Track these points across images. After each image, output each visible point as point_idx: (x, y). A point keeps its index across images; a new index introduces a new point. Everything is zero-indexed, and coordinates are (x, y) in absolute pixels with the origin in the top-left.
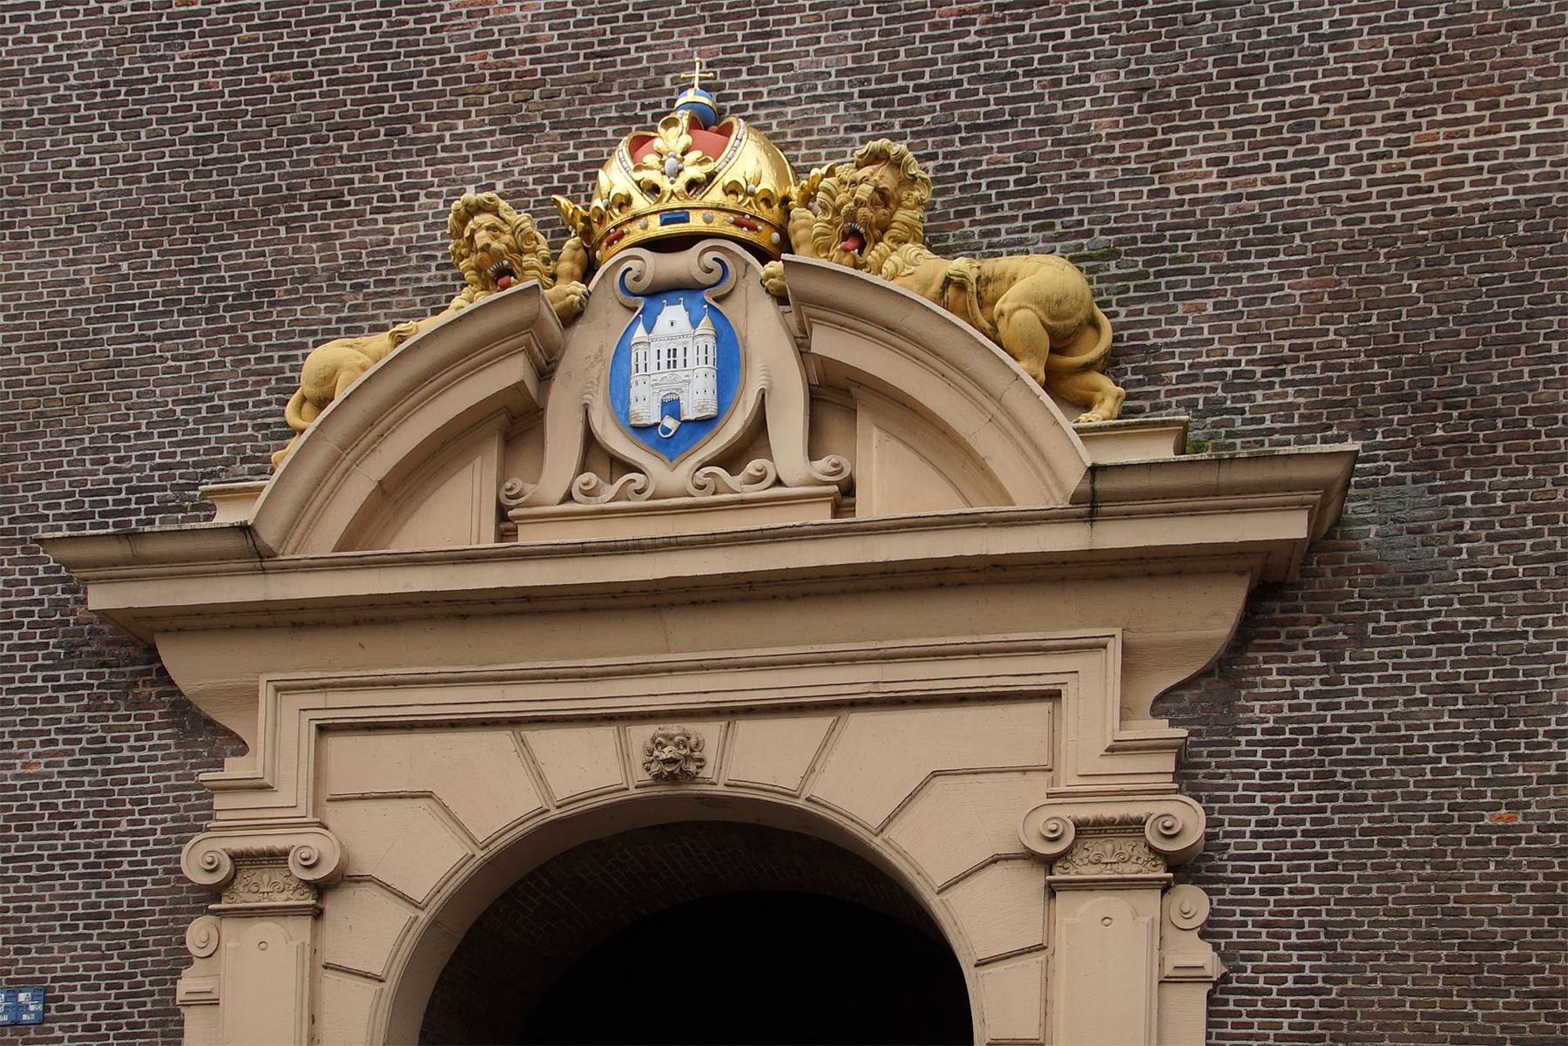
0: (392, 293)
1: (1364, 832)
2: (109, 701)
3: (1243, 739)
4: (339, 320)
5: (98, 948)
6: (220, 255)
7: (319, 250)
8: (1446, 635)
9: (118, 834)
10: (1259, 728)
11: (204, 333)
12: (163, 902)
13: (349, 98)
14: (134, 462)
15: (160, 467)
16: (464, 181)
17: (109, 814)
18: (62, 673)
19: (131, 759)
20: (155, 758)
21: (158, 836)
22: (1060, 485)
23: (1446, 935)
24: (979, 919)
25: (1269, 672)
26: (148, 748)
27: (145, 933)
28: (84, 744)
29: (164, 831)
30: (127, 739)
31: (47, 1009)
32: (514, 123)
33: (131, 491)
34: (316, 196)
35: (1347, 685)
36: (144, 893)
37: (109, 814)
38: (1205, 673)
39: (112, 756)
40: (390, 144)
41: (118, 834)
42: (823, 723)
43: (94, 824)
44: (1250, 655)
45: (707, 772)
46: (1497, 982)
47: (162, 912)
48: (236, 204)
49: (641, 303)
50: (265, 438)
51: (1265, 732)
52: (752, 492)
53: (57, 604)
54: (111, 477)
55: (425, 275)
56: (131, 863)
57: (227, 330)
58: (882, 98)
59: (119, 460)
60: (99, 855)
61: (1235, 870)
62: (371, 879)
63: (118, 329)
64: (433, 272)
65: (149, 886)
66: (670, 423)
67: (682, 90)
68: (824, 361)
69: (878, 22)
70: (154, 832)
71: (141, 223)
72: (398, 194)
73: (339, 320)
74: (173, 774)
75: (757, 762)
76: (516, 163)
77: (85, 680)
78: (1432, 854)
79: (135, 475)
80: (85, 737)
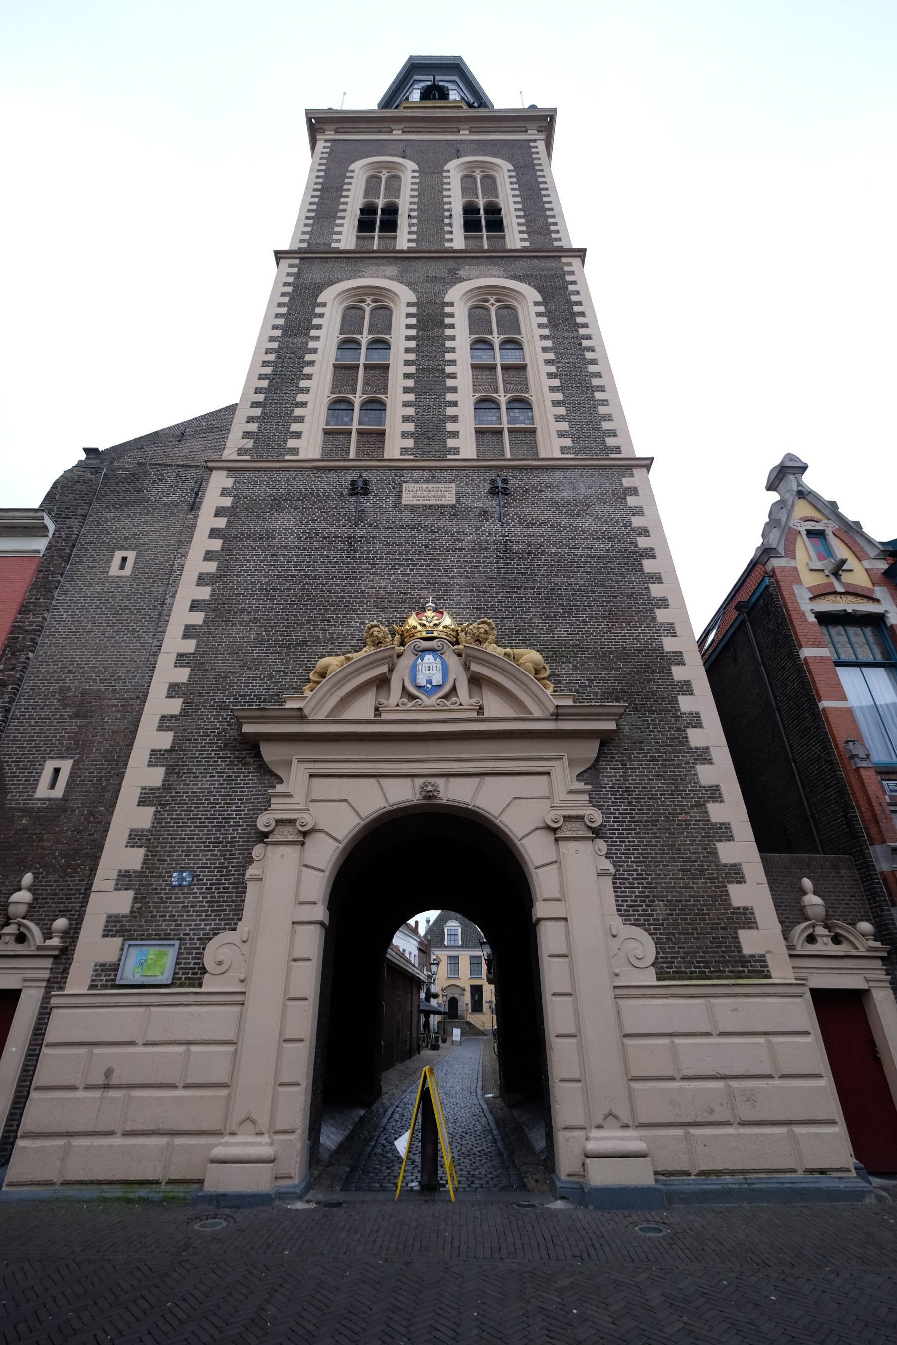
1: (646, 821)
5: (216, 855)
8: (653, 759)
22: (547, 709)
23: (679, 858)
24: (535, 850)
26: (247, 780)
31: (193, 880)
38: (589, 768)
42: (475, 780)
43: (223, 807)
46: (696, 874)
49: (419, 653)
52: (453, 707)
53: (225, 730)
58: (479, 609)
60: (223, 819)
62: (323, 831)
66: (429, 686)
68: (474, 672)
70: (244, 811)
75: (455, 792)
78: (667, 829)
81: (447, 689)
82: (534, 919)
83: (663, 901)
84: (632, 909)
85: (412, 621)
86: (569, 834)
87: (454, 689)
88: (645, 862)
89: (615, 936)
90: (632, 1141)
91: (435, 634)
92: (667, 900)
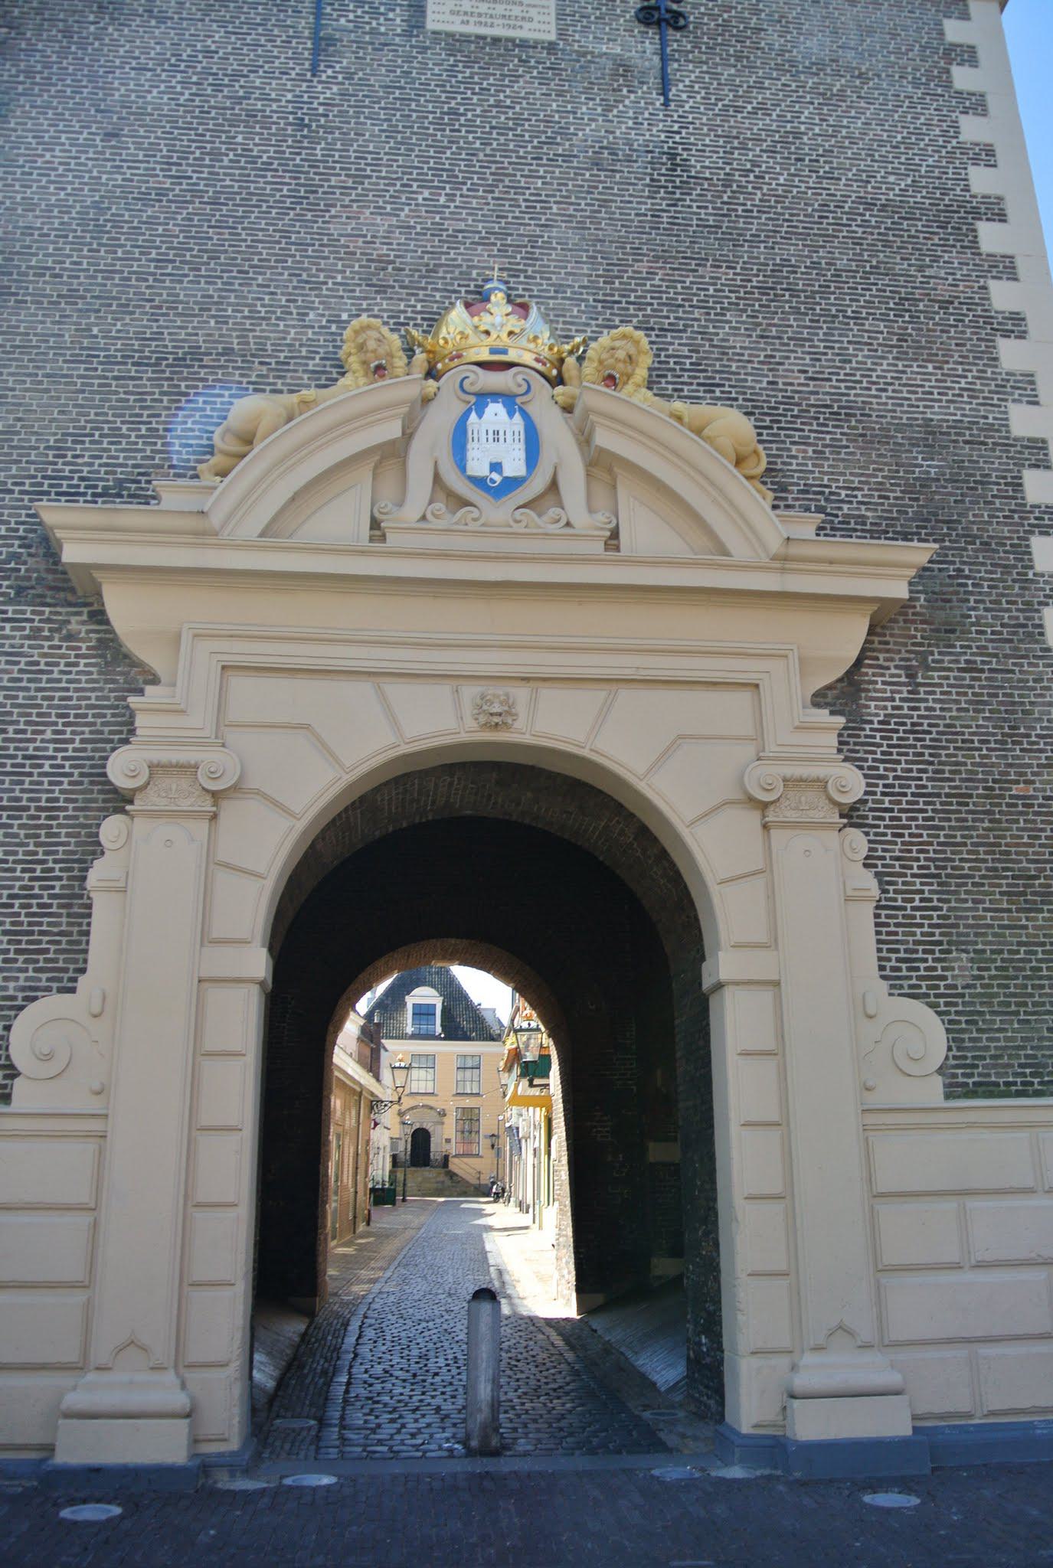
0: (288, 371)
1: (947, 795)
2: (46, 633)
3: (867, 727)
4: (249, 383)
5: (16, 836)
6: (166, 331)
7: (238, 337)
9: (42, 741)
10: (876, 719)
11: (149, 379)
12: (75, 801)
13: (265, 252)
14: (86, 459)
15: (107, 465)
16: (341, 310)
17: (37, 724)
18: (10, 608)
19: (59, 681)
20: (79, 681)
21: (77, 745)
25: (876, 682)
27: (59, 826)
28: (22, 666)
29: (82, 741)
30: (57, 664)
32: (375, 281)
33: (82, 479)
34: (238, 304)
35: (922, 696)
36: (62, 792)
37: (37, 724)
39: (45, 677)
40: (291, 281)
41: (42, 741)
44: (864, 670)
45: (517, 725)
46: (1035, 902)
47: (75, 809)
48: (181, 302)
50: (188, 453)
51: (880, 722)
54: (68, 468)
55: (311, 362)
56: (52, 766)
57: (167, 379)
59: (75, 456)
60: (25, 757)
61: (875, 818)
62: (258, 792)
63: (86, 369)
64: (317, 361)
65: (65, 786)
67: (487, 280)
69: (601, 264)
70: (72, 741)
71: (110, 305)
72: (295, 311)
73: (249, 383)
74: (93, 695)
76: (376, 304)
77: (28, 616)
79: (86, 469)
80: (23, 660)
81: (538, 484)
82: (707, 983)
83: (966, 951)
84: (902, 970)
85: (458, 317)
86: (792, 816)
87: (554, 486)
88: (938, 876)
89: (871, 1017)
90: (874, 1370)
91: (512, 356)
92: (975, 951)
